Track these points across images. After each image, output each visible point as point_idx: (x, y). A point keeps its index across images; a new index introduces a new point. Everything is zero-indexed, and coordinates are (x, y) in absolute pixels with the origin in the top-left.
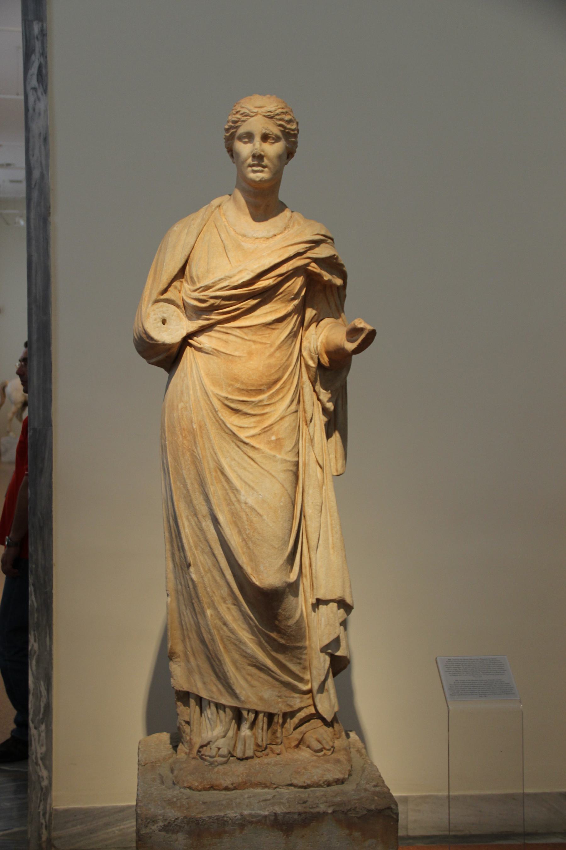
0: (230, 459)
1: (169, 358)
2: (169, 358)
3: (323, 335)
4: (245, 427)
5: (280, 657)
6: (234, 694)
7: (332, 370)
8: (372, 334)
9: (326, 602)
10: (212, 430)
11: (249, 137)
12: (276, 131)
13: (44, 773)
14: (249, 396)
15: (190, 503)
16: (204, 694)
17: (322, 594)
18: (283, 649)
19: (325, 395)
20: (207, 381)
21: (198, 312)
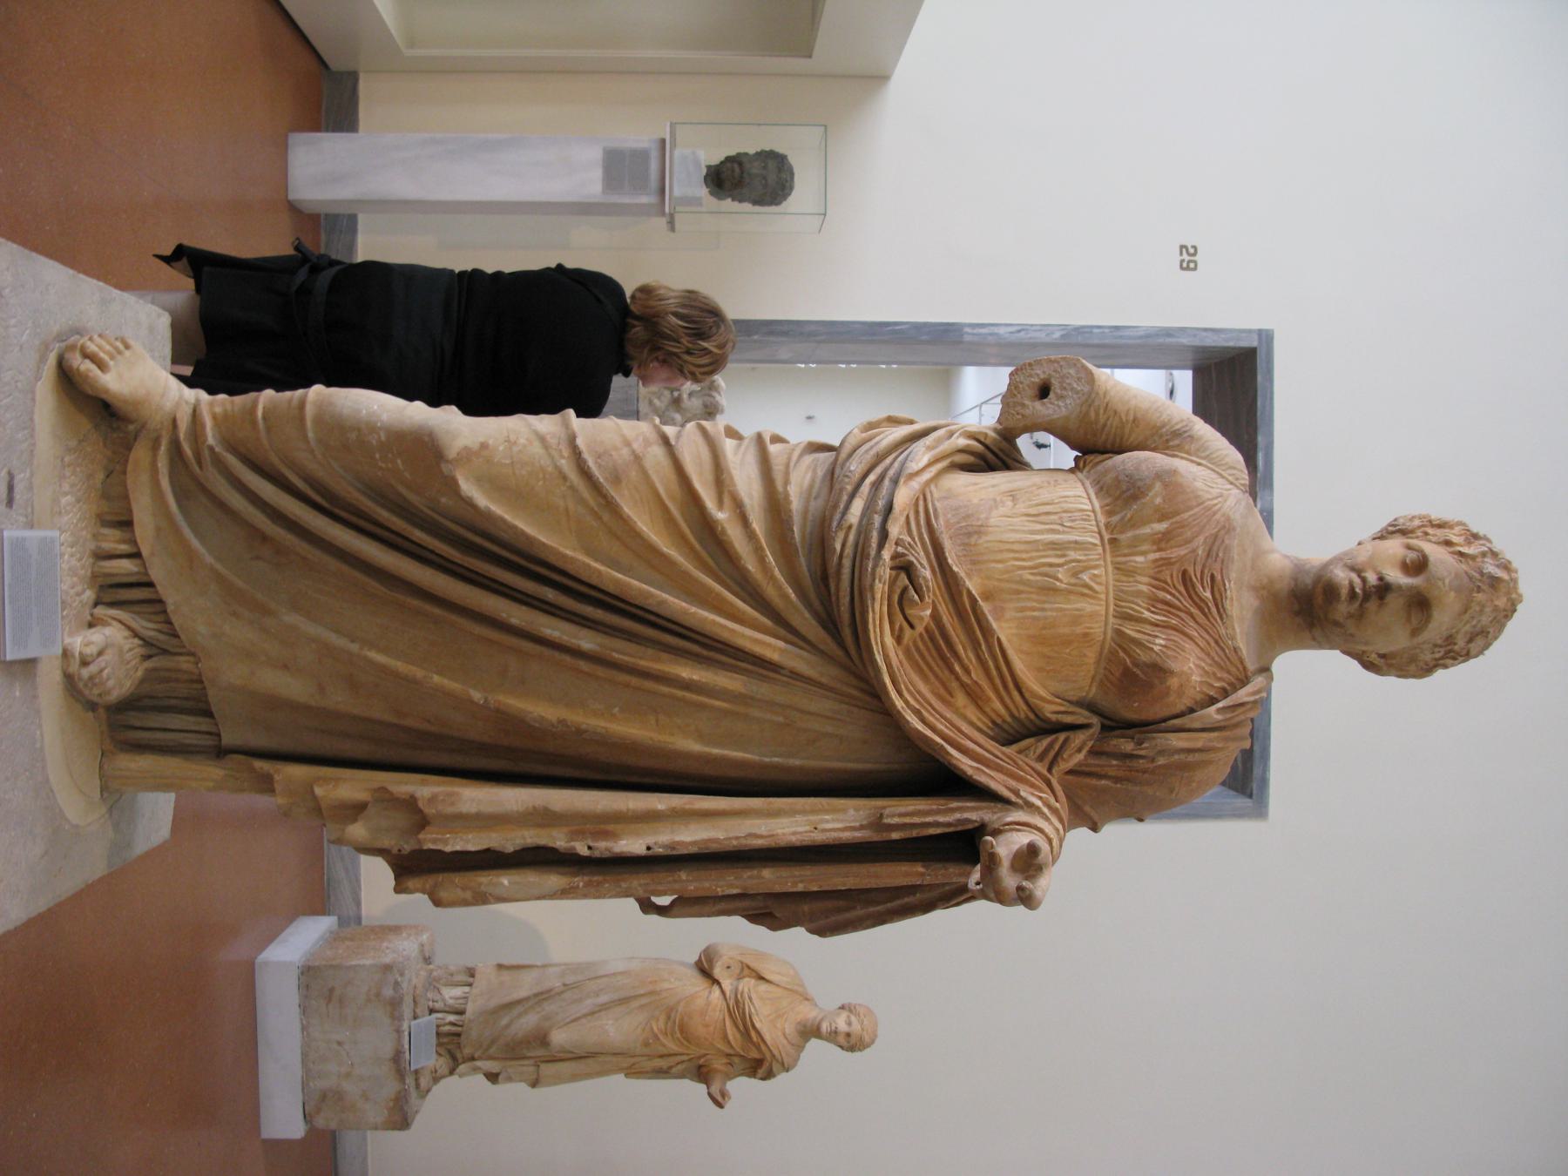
8: (720, 1106)
16: (475, 991)
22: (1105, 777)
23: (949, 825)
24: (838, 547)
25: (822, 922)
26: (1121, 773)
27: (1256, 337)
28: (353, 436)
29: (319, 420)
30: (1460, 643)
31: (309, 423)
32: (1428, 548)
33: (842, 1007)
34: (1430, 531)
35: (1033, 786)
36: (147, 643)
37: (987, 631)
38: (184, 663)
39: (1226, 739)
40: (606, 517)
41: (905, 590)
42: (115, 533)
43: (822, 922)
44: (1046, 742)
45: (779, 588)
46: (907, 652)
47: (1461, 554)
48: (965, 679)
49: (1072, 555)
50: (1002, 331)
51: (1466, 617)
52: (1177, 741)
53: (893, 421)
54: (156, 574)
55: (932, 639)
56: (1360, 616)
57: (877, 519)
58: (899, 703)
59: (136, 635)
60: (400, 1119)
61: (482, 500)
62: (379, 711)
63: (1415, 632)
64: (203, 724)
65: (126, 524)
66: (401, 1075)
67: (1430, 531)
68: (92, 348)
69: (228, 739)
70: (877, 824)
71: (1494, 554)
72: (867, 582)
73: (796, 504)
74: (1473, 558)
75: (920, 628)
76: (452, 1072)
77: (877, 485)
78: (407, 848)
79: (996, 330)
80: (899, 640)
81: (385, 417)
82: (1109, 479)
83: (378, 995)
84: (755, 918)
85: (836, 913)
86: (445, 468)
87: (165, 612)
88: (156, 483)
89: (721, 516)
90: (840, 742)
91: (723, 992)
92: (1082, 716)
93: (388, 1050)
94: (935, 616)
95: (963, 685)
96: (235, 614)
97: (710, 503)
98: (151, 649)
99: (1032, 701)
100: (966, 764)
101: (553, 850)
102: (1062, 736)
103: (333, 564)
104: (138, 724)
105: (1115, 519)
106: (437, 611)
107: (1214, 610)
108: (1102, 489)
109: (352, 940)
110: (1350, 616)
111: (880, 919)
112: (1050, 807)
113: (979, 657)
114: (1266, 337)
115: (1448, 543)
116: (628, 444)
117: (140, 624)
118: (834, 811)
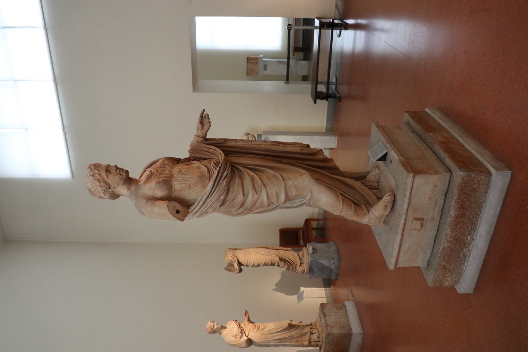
0: (267, 329)
6: (307, 333)
10: (263, 331)
11: (214, 325)
15: (274, 336)
21: (242, 334)
34: (101, 181)
57: (221, 171)
73: (237, 180)
83: (331, 328)
93: (327, 318)
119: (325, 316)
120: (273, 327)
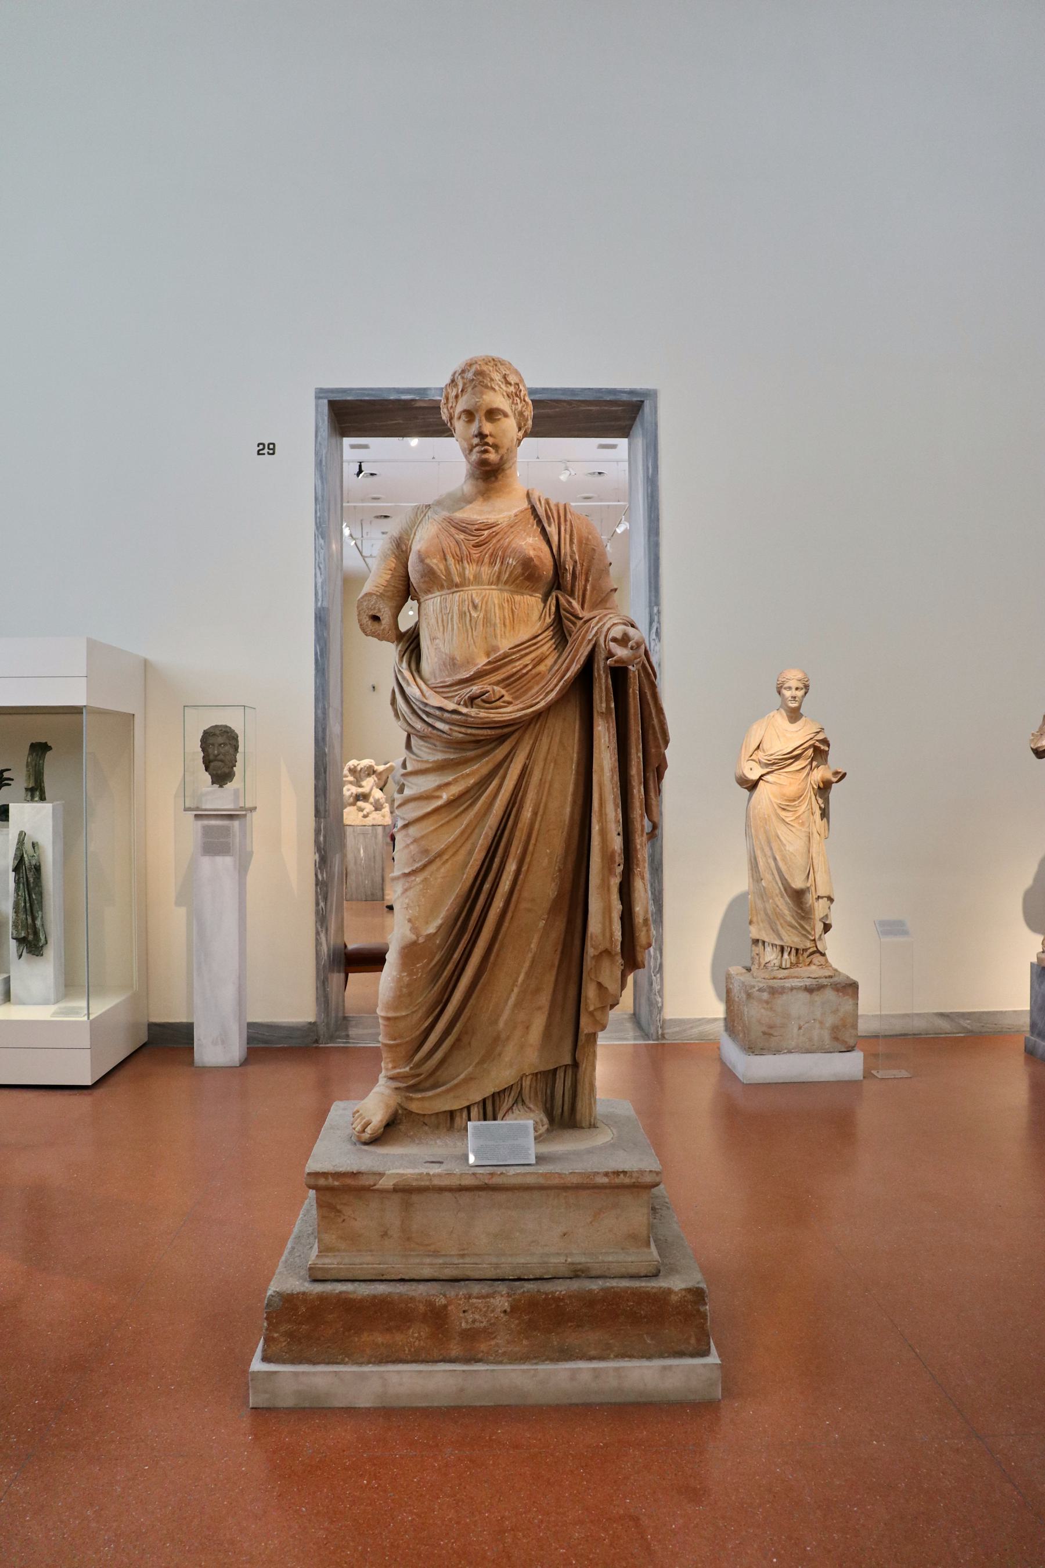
0: (782, 831)
1: (752, 786)
2: (752, 786)
3: (819, 774)
4: (789, 817)
5: (802, 922)
6: (782, 939)
7: (824, 789)
8: (845, 774)
9: (822, 897)
10: (774, 818)
11: (790, 688)
12: (801, 686)
13: (659, 999)
14: (791, 802)
15: (763, 850)
16: (766, 940)
17: (819, 894)
18: (803, 918)
19: (820, 801)
20: (771, 796)
21: (767, 765)
22: (585, 586)
23: (607, 677)
24: (461, 735)
25: (661, 741)
26: (583, 577)
27: (321, 401)
28: (404, 990)
29: (396, 1008)
30: (512, 389)
31: (398, 1014)
32: (459, 409)
33: (779, 693)
34: (450, 405)
35: (587, 632)
36: (516, 1102)
37: (505, 656)
38: (527, 1083)
39: (566, 520)
40: (446, 857)
41: (484, 701)
42: (458, 1120)
43: (661, 741)
44: (565, 621)
45: (482, 767)
46: (516, 698)
47: (462, 391)
48: (530, 667)
49: (465, 608)
50: (319, 580)
51: (497, 388)
52: (566, 549)
53: (393, 702)
54: (479, 1098)
55: (509, 685)
56: (496, 447)
57: (446, 715)
58: (543, 704)
59: (511, 1108)
60: (850, 988)
61: (439, 921)
62: (550, 978)
63: (506, 415)
64: (560, 1074)
65: (452, 1114)
66: (820, 987)
67: (450, 405)
68: (358, 1128)
69: (568, 1060)
70: (605, 715)
71: (463, 372)
72: (480, 721)
73: (440, 756)
74: (464, 384)
75: (503, 692)
76: (823, 955)
77: (428, 714)
78: (619, 960)
79: (319, 585)
80: (509, 703)
81: (395, 973)
82: (423, 586)
83: (767, 1002)
84: (660, 777)
85: (655, 734)
86: (421, 940)
87: (499, 1093)
88: (430, 1098)
89: (445, 796)
90: (564, 734)
91: (768, 773)
92: (552, 601)
93: (804, 996)
94: (497, 683)
95: (534, 667)
96: (500, 1055)
97: (440, 803)
98: (520, 1100)
99: (544, 628)
100: (575, 668)
101: (621, 884)
102: (562, 612)
103: (472, 1001)
104: (560, 1110)
105: (445, 584)
106: (497, 946)
107: (494, 529)
108: (428, 591)
109: (734, 1021)
110: (497, 451)
111: (660, 711)
112: (598, 622)
113: (519, 659)
114: (320, 393)
115: (457, 397)
116: (408, 846)
117: (505, 1107)
118: (600, 738)
119: (809, 990)
120: (790, 848)
